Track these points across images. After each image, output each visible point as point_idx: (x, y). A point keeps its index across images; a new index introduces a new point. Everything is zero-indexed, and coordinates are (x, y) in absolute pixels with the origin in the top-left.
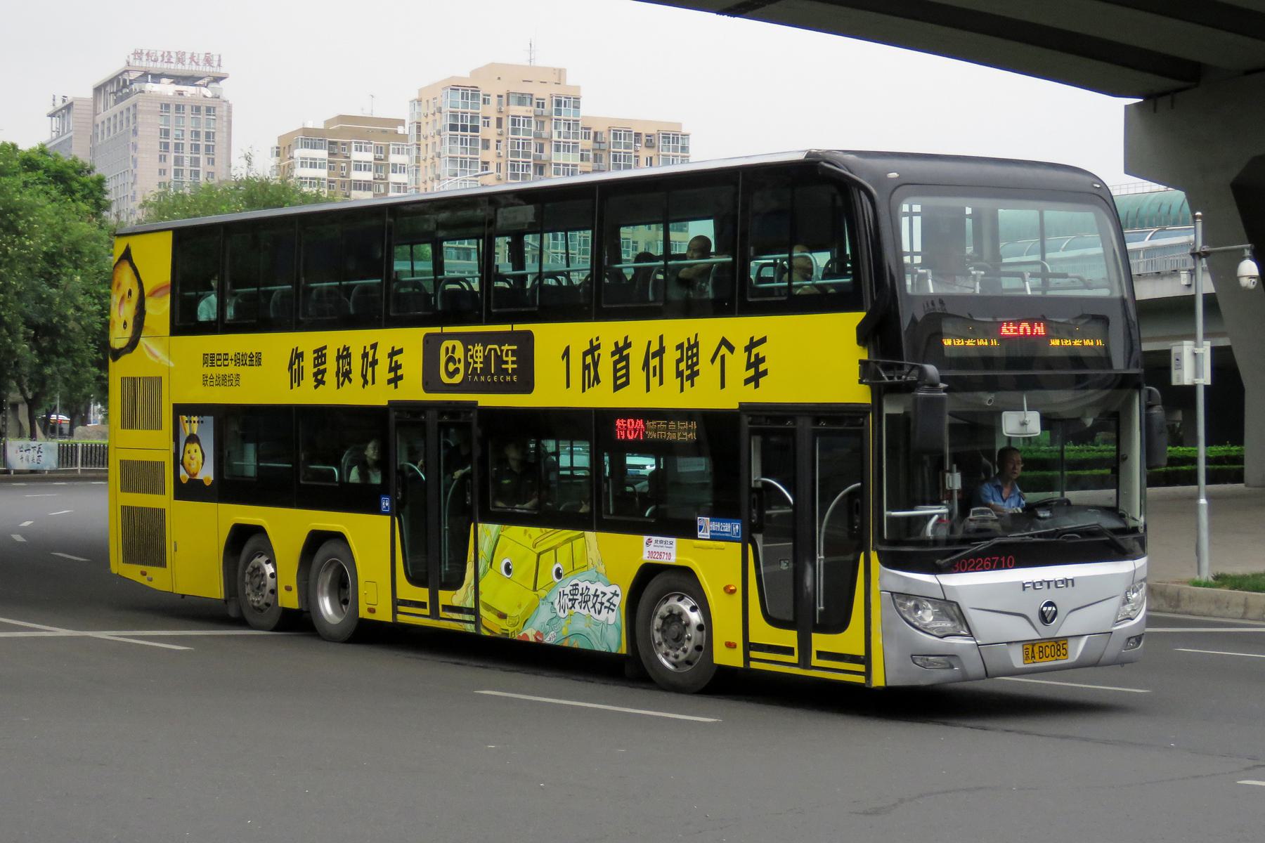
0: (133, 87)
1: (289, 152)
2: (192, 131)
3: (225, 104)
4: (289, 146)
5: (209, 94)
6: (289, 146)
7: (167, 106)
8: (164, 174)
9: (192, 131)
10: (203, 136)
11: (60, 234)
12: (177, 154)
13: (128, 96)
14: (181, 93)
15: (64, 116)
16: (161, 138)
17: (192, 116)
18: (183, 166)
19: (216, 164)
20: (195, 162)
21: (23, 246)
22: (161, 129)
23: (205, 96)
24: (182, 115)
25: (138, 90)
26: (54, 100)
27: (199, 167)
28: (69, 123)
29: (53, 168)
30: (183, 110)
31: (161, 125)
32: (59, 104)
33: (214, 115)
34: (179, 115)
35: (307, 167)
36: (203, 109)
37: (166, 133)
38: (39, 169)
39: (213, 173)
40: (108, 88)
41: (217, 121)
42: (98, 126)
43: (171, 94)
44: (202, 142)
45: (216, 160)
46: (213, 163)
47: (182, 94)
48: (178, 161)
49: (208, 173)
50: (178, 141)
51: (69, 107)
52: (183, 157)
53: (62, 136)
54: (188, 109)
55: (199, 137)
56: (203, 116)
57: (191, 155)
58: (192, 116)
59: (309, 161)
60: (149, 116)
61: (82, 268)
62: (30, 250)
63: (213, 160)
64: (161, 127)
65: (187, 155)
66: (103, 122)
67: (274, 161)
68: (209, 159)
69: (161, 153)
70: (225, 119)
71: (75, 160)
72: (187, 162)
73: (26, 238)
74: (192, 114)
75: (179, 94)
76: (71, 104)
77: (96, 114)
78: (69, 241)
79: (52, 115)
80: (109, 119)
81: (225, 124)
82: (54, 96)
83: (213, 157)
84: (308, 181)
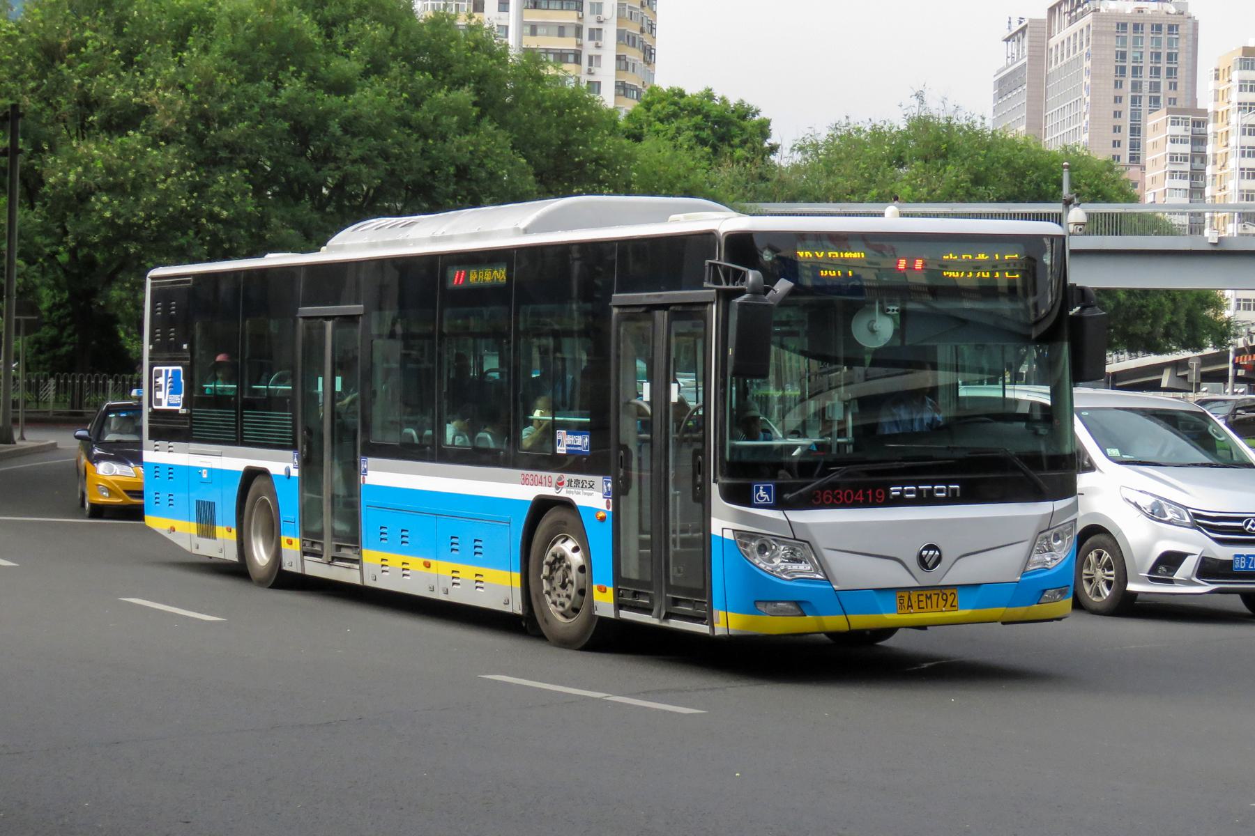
0: (1086, 6)
1: (1229, 75)
2: (1152, 53)
3: (1189, 20)
4: (1229, 67)
5: (1173, 10)
6: (1229, 67)
7: (1124, 25)
8: (1120, 102)
9: (1152, 53)
10: (1164, 57)
12: (1133, 79)
13: (1083, 14)
14: (1140, 11)
15: (1019, 41)
16: (1117, 61)
17: (1152, 36)
18: (1141, 92)
19: (1178, 88)
20: (1155, 87)
22: (1117, 52)
23: (1168, 13)
24: (1142, 35)
25: (1092, 9)
26: (1010, 22)
27: (1159, 92)
28: (1023, 47)
29: (714, 113)
30: (1142, 29)
31: (1117, 47)
32: (1016, 27)
33: (1176, 34)
34: (1137, 35)
35: (1246, 91)
36: (1165, 29)
37: (1123, 56)
38: (699, 114)
39: (1175, 99)
40: (1063, 8)
41: (1180, 40)
42: (1051, 50)
43: (1129, 11)
44: (1164, 65)
45: (1179, 84)
46: (1175, 88)
47: (1142, 12)
48: (1136, 86)
49: (1170, 99)
50: (1135, 64)
51: (1023, 30)
52: (1141, 82)
53: (1016, 62)
54: (1147, 28)
55: (1125, 58)
56: (1164, 36)
57: (1152, 80)
58: (1152, 36)
59: (1249, 84)
60: (1104, 38)
63: (1175, 84)
64: (1117, 49)
65: (1146, 79)
66: (1057, 46)
67: (1212, 85)
68: (1170, 83)
69: (1117, 79)
70: (1190, 37)
71: (741, 104)
72: (1146, 87)
73: (606, 187)
74: (1152, 33)
75: (1139, 11)
76: (1026, 26)
77: (1050, 37)
78: (680, 188)
79: (1007, 40)
80: (1063, 42)
81: (1190, 43)
82: (1010, 18)
83: (1175, 80)
84: (1248, 106)
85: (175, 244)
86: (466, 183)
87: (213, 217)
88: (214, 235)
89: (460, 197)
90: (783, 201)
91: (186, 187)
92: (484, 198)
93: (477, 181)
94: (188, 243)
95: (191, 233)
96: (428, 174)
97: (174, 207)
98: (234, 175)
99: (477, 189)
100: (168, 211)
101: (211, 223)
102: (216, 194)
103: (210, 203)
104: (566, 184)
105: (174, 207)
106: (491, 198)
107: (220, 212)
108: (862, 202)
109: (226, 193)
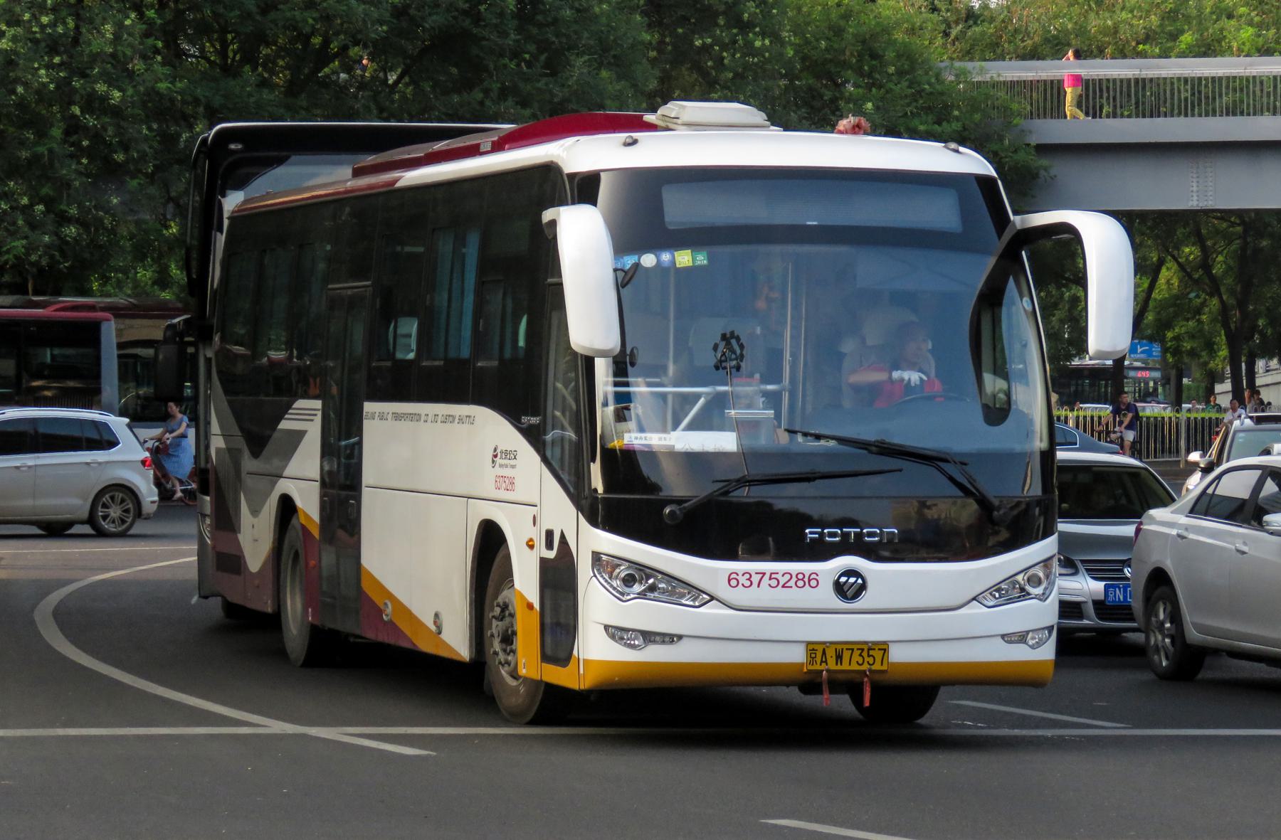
11: (842, 23)
21: (749, 49)
61: (880, 87)
62: (764, 57)
78: (855, 36)
85: (24, 154)
86: (535, 31)
87: (94, 103)
88: (96, 136)
89: (527, 56)
90: (1023, 57)
91: (43, 44)
92: (572, 58)
93: (555, 21)
94: (51, 151)
95: (57, 132)
96: (465, 13)
97: (26, 85)
98: (128, 22)
99: (554, 39)
100: (14, 92)
101: (92, 113)
102: (95, 58)
103: (84, 75)
104: (680, 31)
105: (26, 85)
106: (586, 57)
107: (107, 92)
108: (1167, 57)
109: (113, 55)
